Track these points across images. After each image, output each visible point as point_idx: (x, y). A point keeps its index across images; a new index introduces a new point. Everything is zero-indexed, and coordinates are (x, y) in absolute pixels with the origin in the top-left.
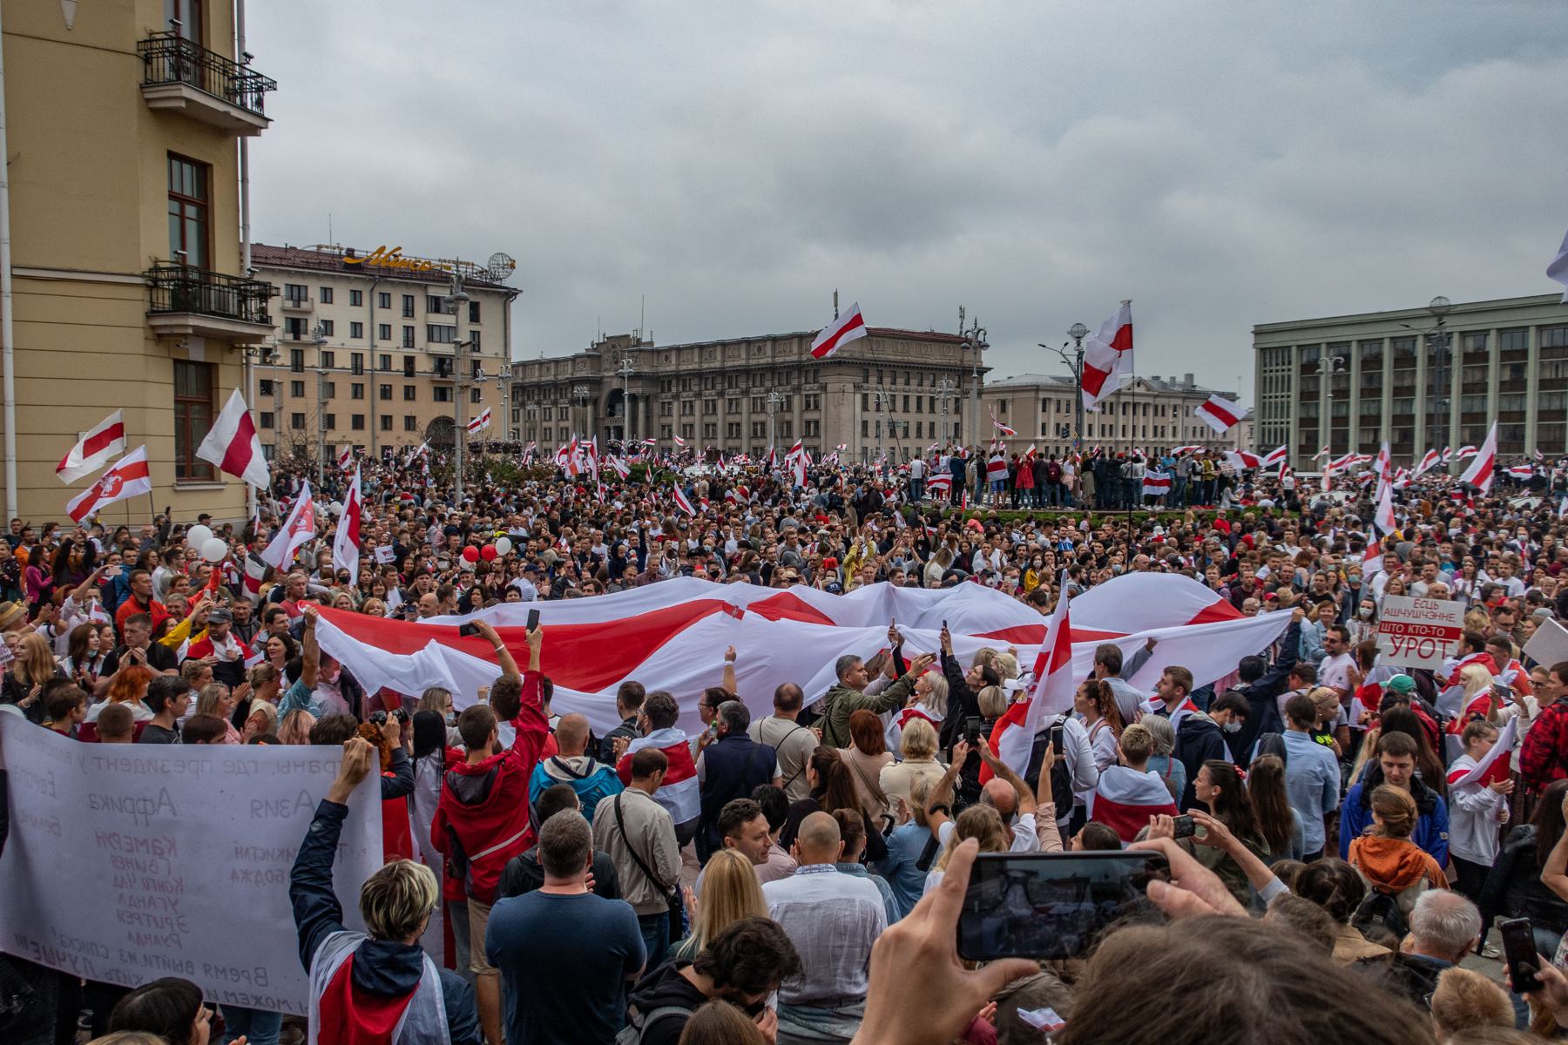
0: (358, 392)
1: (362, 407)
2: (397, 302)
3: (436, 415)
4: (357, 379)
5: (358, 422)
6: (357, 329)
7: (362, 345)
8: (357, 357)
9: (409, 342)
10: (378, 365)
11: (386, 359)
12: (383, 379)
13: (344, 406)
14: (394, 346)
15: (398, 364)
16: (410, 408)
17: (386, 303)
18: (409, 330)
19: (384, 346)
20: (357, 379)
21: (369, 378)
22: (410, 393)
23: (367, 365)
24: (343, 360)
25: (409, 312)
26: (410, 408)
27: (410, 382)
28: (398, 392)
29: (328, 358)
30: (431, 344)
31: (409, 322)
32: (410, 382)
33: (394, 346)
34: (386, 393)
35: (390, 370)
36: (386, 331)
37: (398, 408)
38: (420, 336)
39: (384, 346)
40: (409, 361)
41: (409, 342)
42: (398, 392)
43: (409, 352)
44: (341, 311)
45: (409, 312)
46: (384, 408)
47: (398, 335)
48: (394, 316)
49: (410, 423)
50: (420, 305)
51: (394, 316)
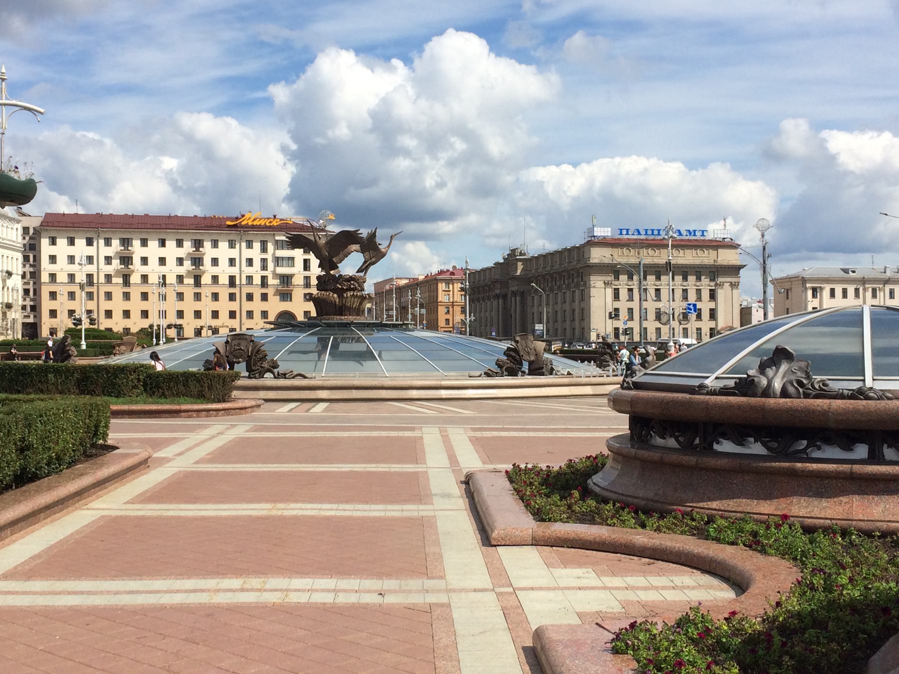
0: (232, 297)
1: (235, 306)
2: (257, 246)
3: (282, 309)
4: (232, 290)
5: (232, 315)
6: (232, 262)
7: (234, 271)
8: (232, 279)
9: (264, 267)
10: (244, 281)
11: (250, 278)
12: (246, 290)
13: (224, 306)
14: (256, 271)
15: (257, 280)
16: (264, 306)
17: (250, 245)
18: (264, 261)
19: (248, 271)
20: (232, 290)
21: (239, 288)
22: (264, 297)
23: (238, 282)
24: (224, 280)
25: (264, 250)
26: (264, 306)
27: (264, 291)
28: (257, 297)
29: (215, 279)
30: (277, 268)
31: (264, 256)
32: (264, 291)
33: (256, 271)
34: (250, 297)
35: (252, 284)
36: (250, 262)
37: (257, 306)
38: (271, 265)
39: (248, 271)
40: (264, 279)
41: (264, 267)
42: (257, 297)
43: (264, 273)
44: (224, 251)
45: (264, 250)
46: (247, 306)
47: (257, 264)
48: (255, 253)
49: (265, 314)
50: (270, 247)
51: (255, 253)
